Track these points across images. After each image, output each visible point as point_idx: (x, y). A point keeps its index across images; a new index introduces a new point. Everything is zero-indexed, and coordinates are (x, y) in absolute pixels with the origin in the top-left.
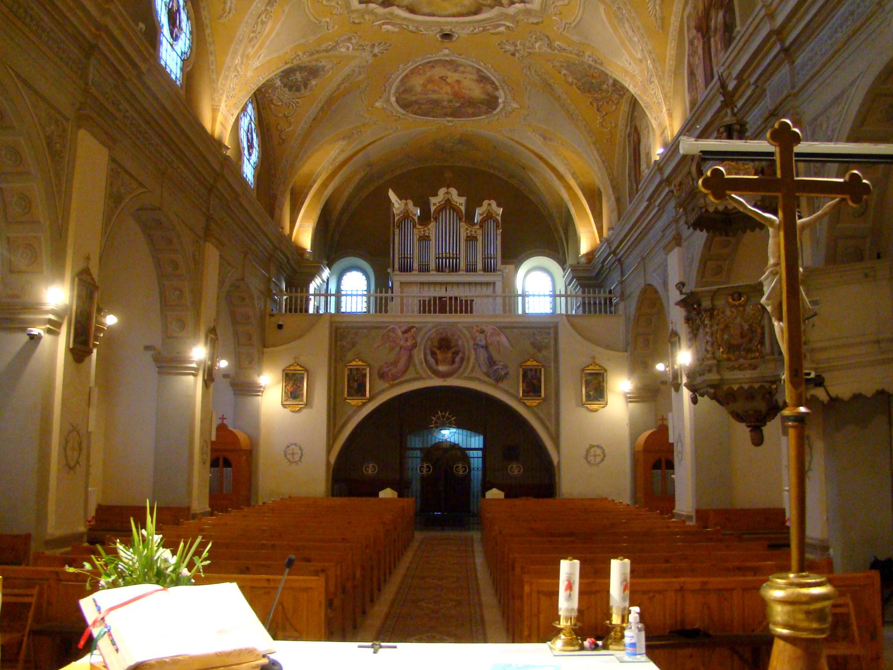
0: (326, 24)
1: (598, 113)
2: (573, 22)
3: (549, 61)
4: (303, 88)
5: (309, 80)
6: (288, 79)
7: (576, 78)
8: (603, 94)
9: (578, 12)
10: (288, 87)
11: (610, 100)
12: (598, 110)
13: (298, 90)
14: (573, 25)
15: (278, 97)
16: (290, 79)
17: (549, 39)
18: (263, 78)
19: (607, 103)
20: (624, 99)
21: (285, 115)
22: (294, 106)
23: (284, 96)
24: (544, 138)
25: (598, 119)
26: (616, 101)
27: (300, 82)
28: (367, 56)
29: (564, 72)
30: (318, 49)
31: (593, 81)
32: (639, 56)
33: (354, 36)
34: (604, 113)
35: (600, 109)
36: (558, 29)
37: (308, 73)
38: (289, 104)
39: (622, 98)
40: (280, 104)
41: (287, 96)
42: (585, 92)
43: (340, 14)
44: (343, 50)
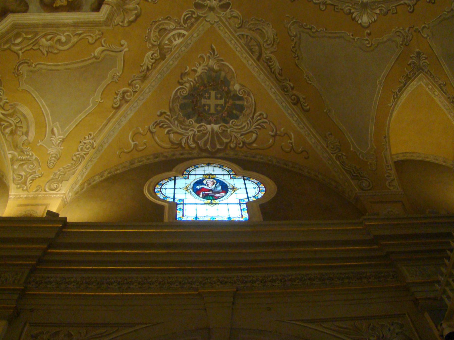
0: (105, 53)
4: (238, 102)
5: (229, 92)
6: (212, 114)
10: (228, 119)
13: (241, 108)
15: (241, 135)
16: (212, 111)
18: (93, 139)
21: (272, 136)
22: (265, 120)
23: (245, 127)
27: (226, 102)
28: (211, 16)
30: (145, 68)
33: (160, 25)
37: (214, 90)
38: (258, 125)
40: (254, 136)
41: (244, 124)
43: (102, 34)
44: (178, 41)
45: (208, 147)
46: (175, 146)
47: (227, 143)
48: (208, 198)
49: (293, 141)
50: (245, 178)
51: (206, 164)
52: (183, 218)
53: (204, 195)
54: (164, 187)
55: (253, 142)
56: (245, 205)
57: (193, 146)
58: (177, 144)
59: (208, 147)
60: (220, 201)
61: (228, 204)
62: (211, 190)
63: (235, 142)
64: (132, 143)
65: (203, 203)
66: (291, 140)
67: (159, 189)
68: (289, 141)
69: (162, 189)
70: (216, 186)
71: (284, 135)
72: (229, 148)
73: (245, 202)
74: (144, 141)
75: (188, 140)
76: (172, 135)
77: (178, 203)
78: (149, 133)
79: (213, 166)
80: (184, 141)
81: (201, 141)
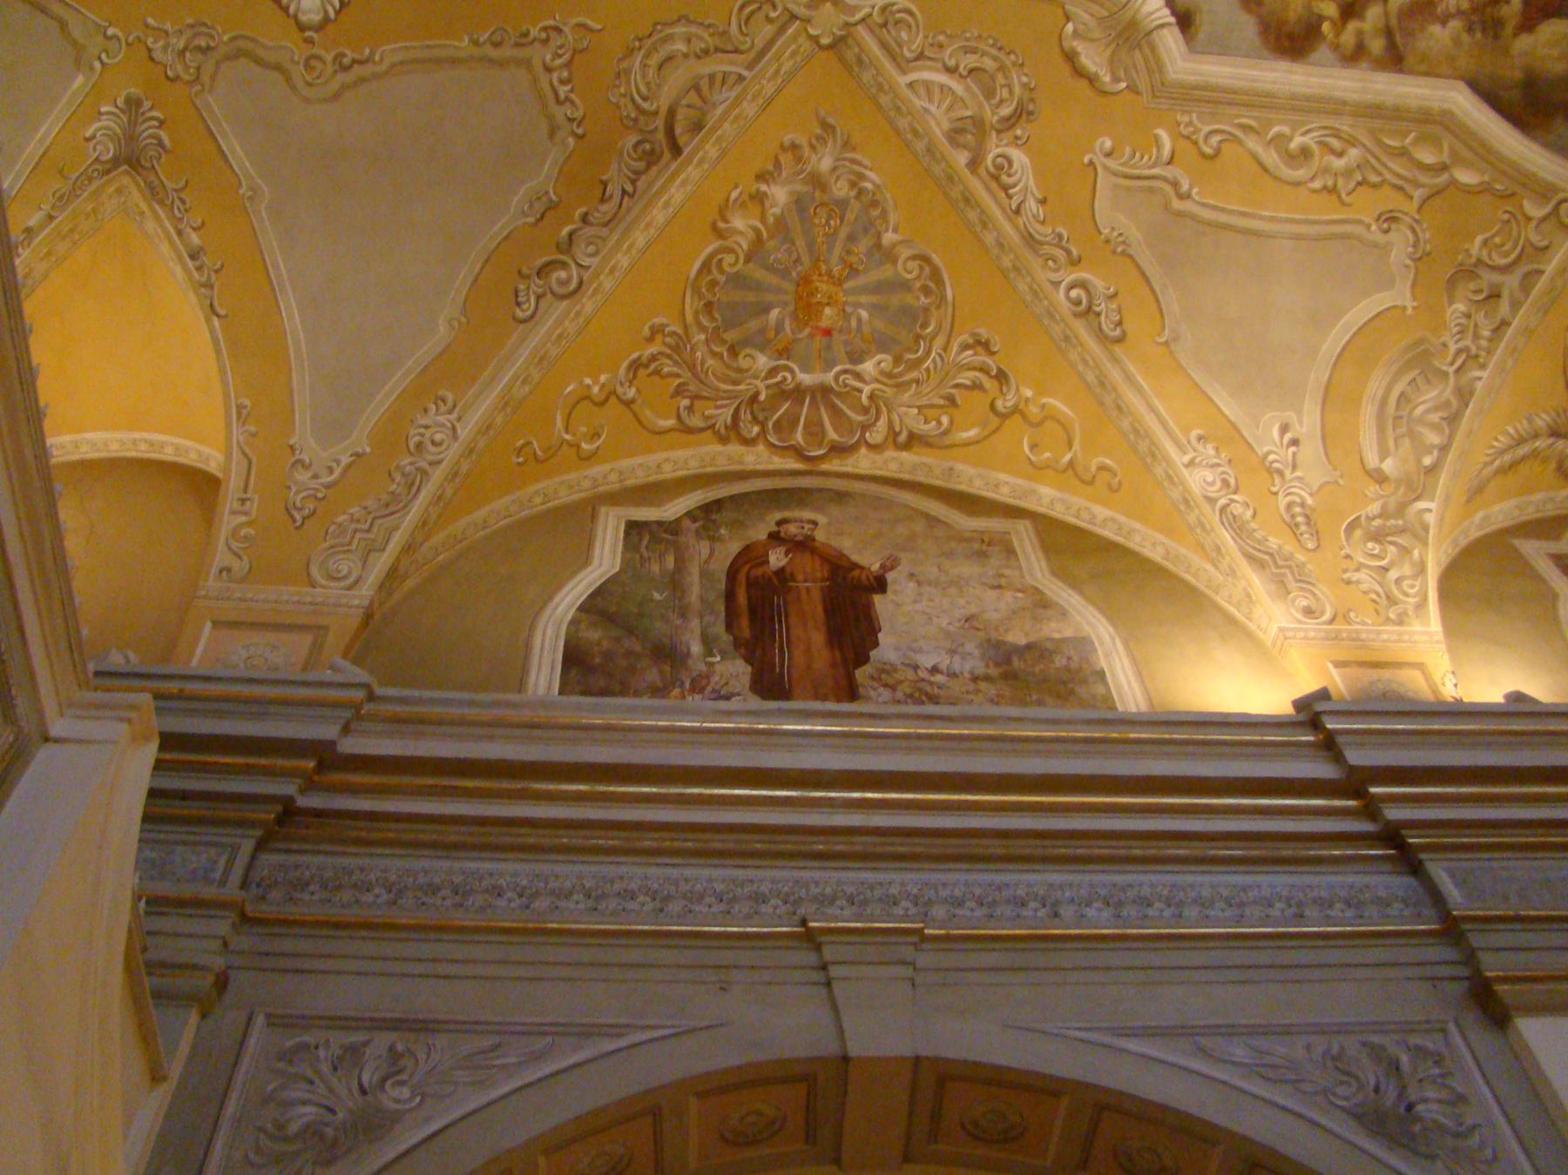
1: (622, 370)
2: (1204, 205)
3: (826, 126)
7: (758, 240)
8: (710, 362)
9: (1272, 219)
11: (696, 397)
12: (636, 366)
14: (1177, 204)
17: (1009, 123)
19: (679, 391)
20: (719, 448)
24: (130, 159)
25: (596, 381)
26: (696, 422)
29: (780, 195)
31: (774, 314)
32: (1388, 466)
34: (631, 393)
35: (642, 372)
36: (1108, 155)
39: (724, 440)
42: (696, 291)
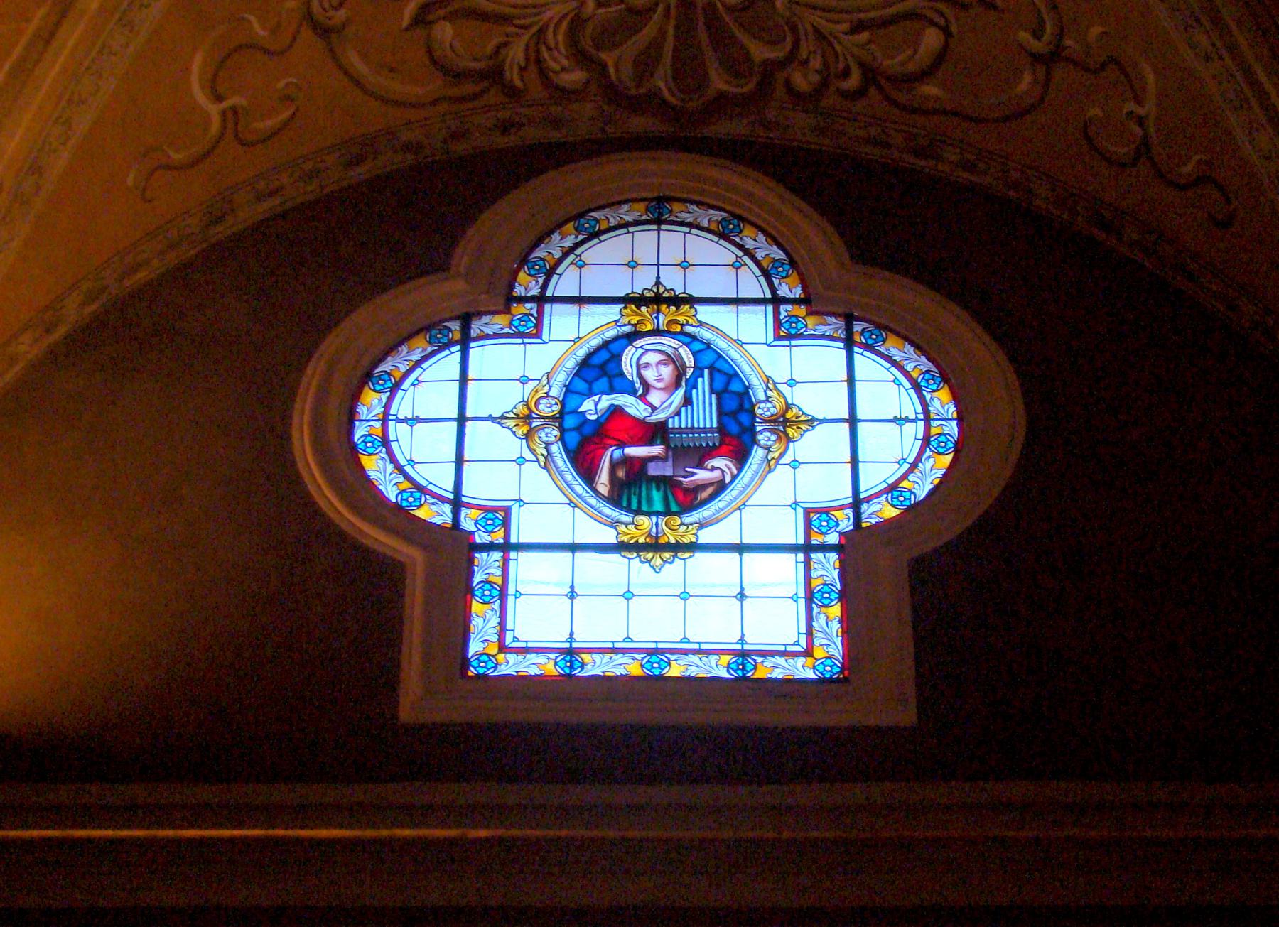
15: (857, 28)
21: (1036, 58)
40: (931, 39)
45: (661, 81)
46: (468, 88)
47: (770, 69)
48: (639, 503)
49: (1149, 108)
50: (858, 327)
51: (641, 206)
52: (501, 657)
53: (621, 473)
54: (402, 406)
55: (925, 75)
56: (833, 557)
57: (574, 77)
58: (482, 76)
59: (661, 84)
60: (701, 525)
61: (740, 548)
62: (655, 432)
63: (816, 63)
64: (214, 110)
65: (609, 537)
66: (1139, 101)
67: (378, 425)
68: (1130, 106)
69: (391, 424)
70: (687, 401)
71: (1103, 66)
72: (780, 92)
73: (833, 539)
74: (281, 84)
75: (543, 49)
76: (445, 32)
77: (481, 538)
78: (307, 34)
79: (682, 224)
80: (517, 53)
81: (617, 52)
